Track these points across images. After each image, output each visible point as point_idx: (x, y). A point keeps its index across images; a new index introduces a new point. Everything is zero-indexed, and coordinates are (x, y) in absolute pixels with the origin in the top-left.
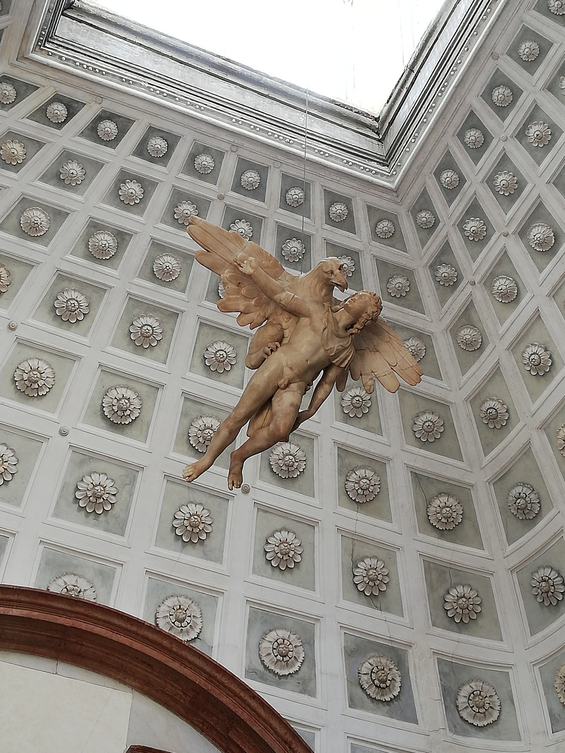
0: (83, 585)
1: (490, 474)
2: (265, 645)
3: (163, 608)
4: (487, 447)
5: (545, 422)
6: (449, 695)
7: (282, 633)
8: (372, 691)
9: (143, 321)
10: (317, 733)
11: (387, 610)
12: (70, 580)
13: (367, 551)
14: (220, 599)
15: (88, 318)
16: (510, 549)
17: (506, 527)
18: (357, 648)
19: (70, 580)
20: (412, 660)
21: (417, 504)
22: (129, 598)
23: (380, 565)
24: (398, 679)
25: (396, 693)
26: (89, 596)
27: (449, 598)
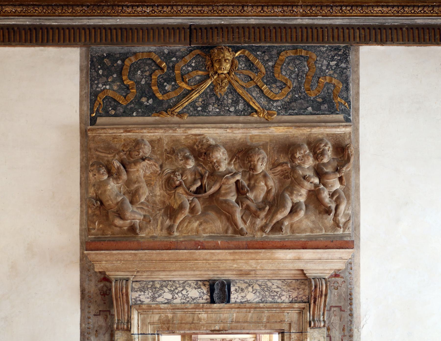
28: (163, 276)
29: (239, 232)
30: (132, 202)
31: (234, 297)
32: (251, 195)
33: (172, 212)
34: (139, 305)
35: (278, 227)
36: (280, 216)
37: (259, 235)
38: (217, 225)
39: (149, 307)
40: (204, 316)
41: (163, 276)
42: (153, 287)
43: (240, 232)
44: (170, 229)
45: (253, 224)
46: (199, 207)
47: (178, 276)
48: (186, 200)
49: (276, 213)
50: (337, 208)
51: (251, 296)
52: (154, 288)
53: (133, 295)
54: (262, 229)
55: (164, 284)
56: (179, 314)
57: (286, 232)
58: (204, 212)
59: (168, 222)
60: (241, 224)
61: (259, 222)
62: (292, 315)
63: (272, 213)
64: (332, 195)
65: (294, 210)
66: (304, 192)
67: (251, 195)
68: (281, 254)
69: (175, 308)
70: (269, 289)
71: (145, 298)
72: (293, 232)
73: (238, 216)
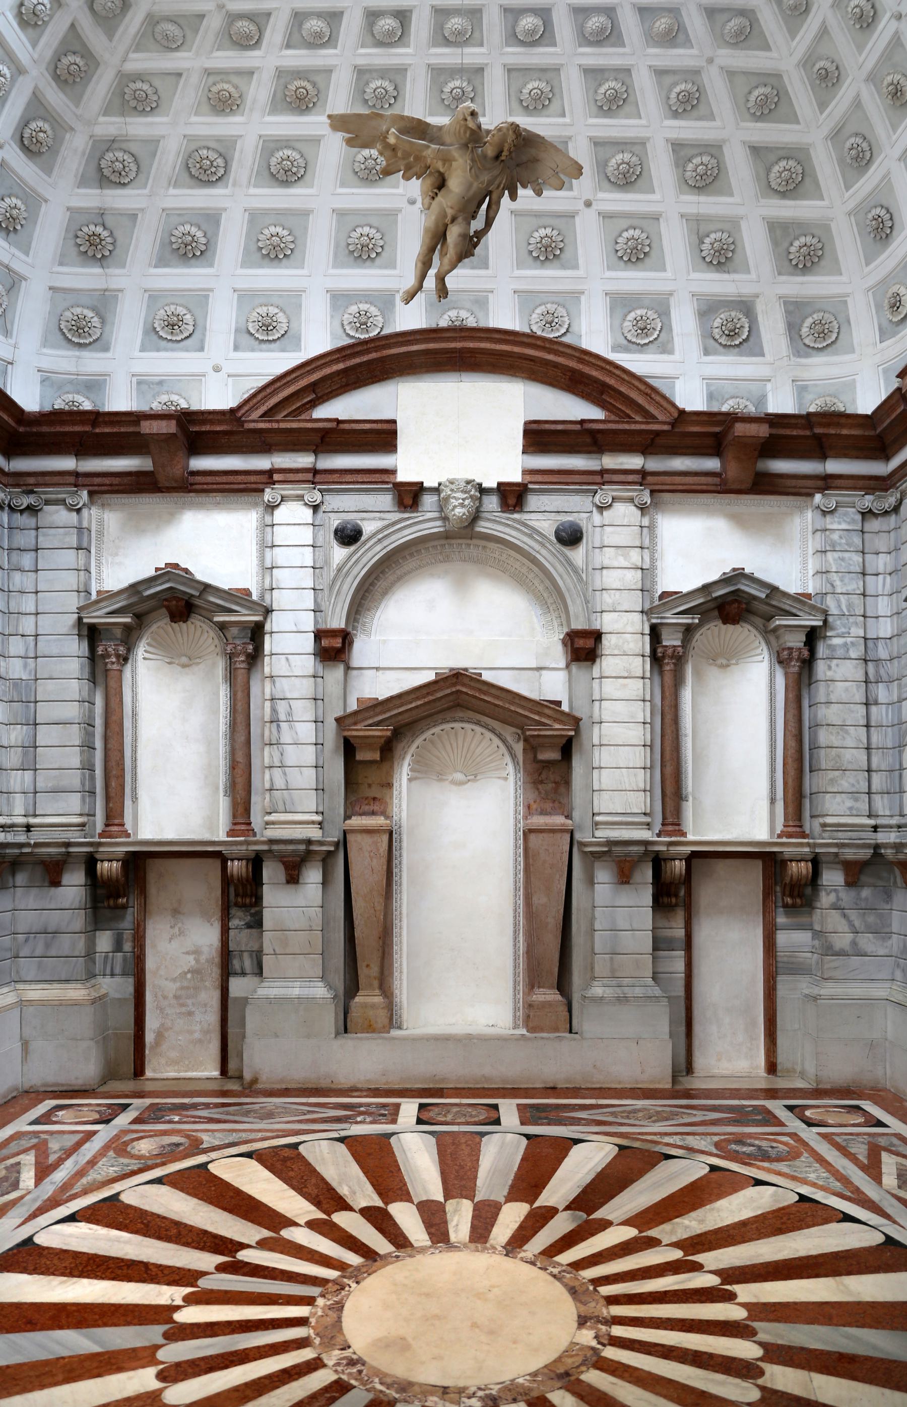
0: (464, 314)
1: (825, 130)
2: (627, 324)
3: (534, 316)
4: (822, 105)
5: (871, 73)
6: (793, 329)
7: (639, 312)
8: (723, 340)
9: (451, 85)
10: (676, 381)
11: (735, 271)
12: (453, 314)
13: (712, 227)
14: (583, 298)
15: (399, 99)
16: (847, 195)
17: (843, 176)
18: (707, 309)
19: (453, 314)
20: (760, 307)
21: (757, 174)
22: (504, 316)
23: (725, 235)
24: (747, 325)
25: (744, 337)
26: (471, 323)
27: (793, 249)
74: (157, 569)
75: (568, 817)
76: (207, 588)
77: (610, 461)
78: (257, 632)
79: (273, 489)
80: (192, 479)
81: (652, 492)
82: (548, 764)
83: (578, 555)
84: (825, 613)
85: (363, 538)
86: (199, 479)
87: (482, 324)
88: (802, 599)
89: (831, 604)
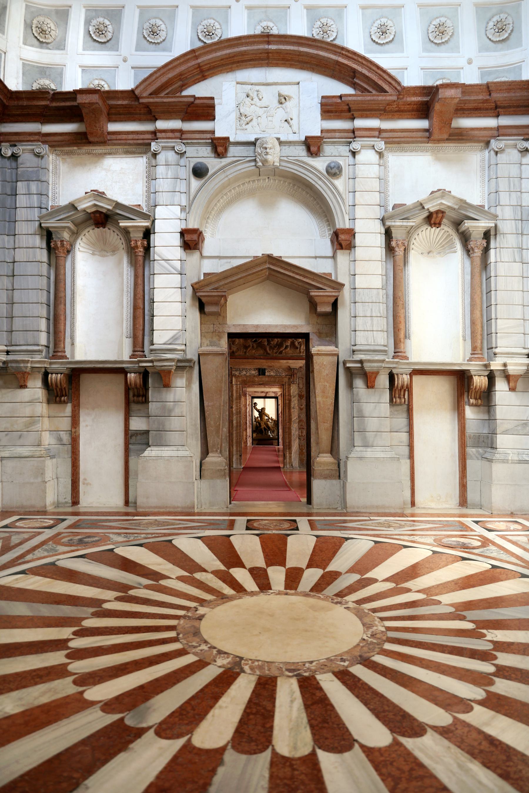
28: (243, 367)
29: (268, 353)
30: (233, 344)
31: (266, 374)
32: (272, 343)
33: (246, 347)
34: (235, 376)
35: (281, 353)
36: (281, 349)
37: (275, 355)
38: (261, 352)
39: (238, 376)
40: (256, 379)
41: (243, 367)
42: (240, 370)
43: (269, 354)
44: (245, 352)
45: (273, 351)
46: (255, 346)
47: (248, 367)
48: (251, 344)
49: (280, 348)
50: (300, 347)
51: (272, 374)
52: (240, 370)
53: (233, 372)
54: (276, 353)
55: (243, 369)
56: (248, 378)
57: (284, 354)
58: (257, 348)
59: (245, 350)
60: (269, 352)
61: (275, 351)
62: (286, 380)
63: (279, 348)
64: (299, 343)
65: (286, 347)
66: (289, 342)
67: (272, 343)
68: (282, 361)
69: (247, 377)
70: (278, 372)
71: (237, 373)
72: (286, 354)
73: (268, 349)
74: (86, 193)
75: (337, 347)
76: (118, 205)
77: (359, 123)
78: (148, 233)
79: (156, 142)
80: (109, 137)
81: (386, 143)
82: (325, 315)
83: (339, 183)
84: (495, 217)
85: (210, 173)
86: (114, 137)
87: (282, 32)
88: (480, 209)
89: (499, 211)
